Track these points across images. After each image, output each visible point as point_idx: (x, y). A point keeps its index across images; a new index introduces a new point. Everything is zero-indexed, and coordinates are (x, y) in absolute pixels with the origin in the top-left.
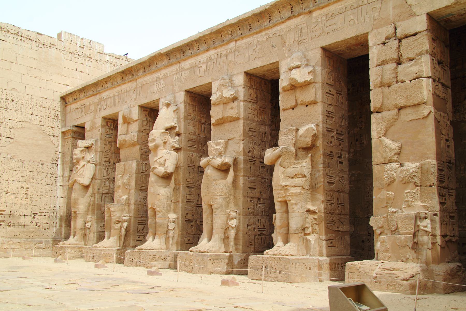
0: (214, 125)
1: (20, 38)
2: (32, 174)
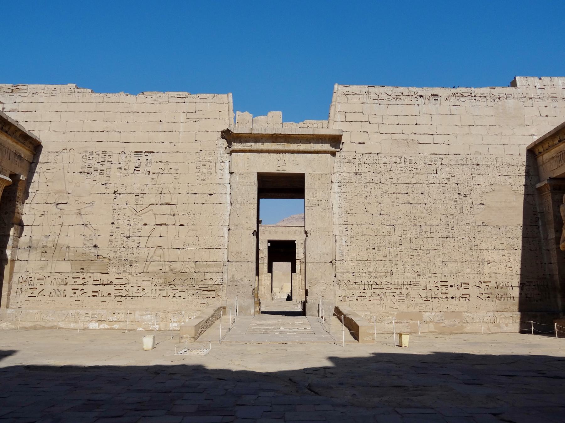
1: (474, 98)
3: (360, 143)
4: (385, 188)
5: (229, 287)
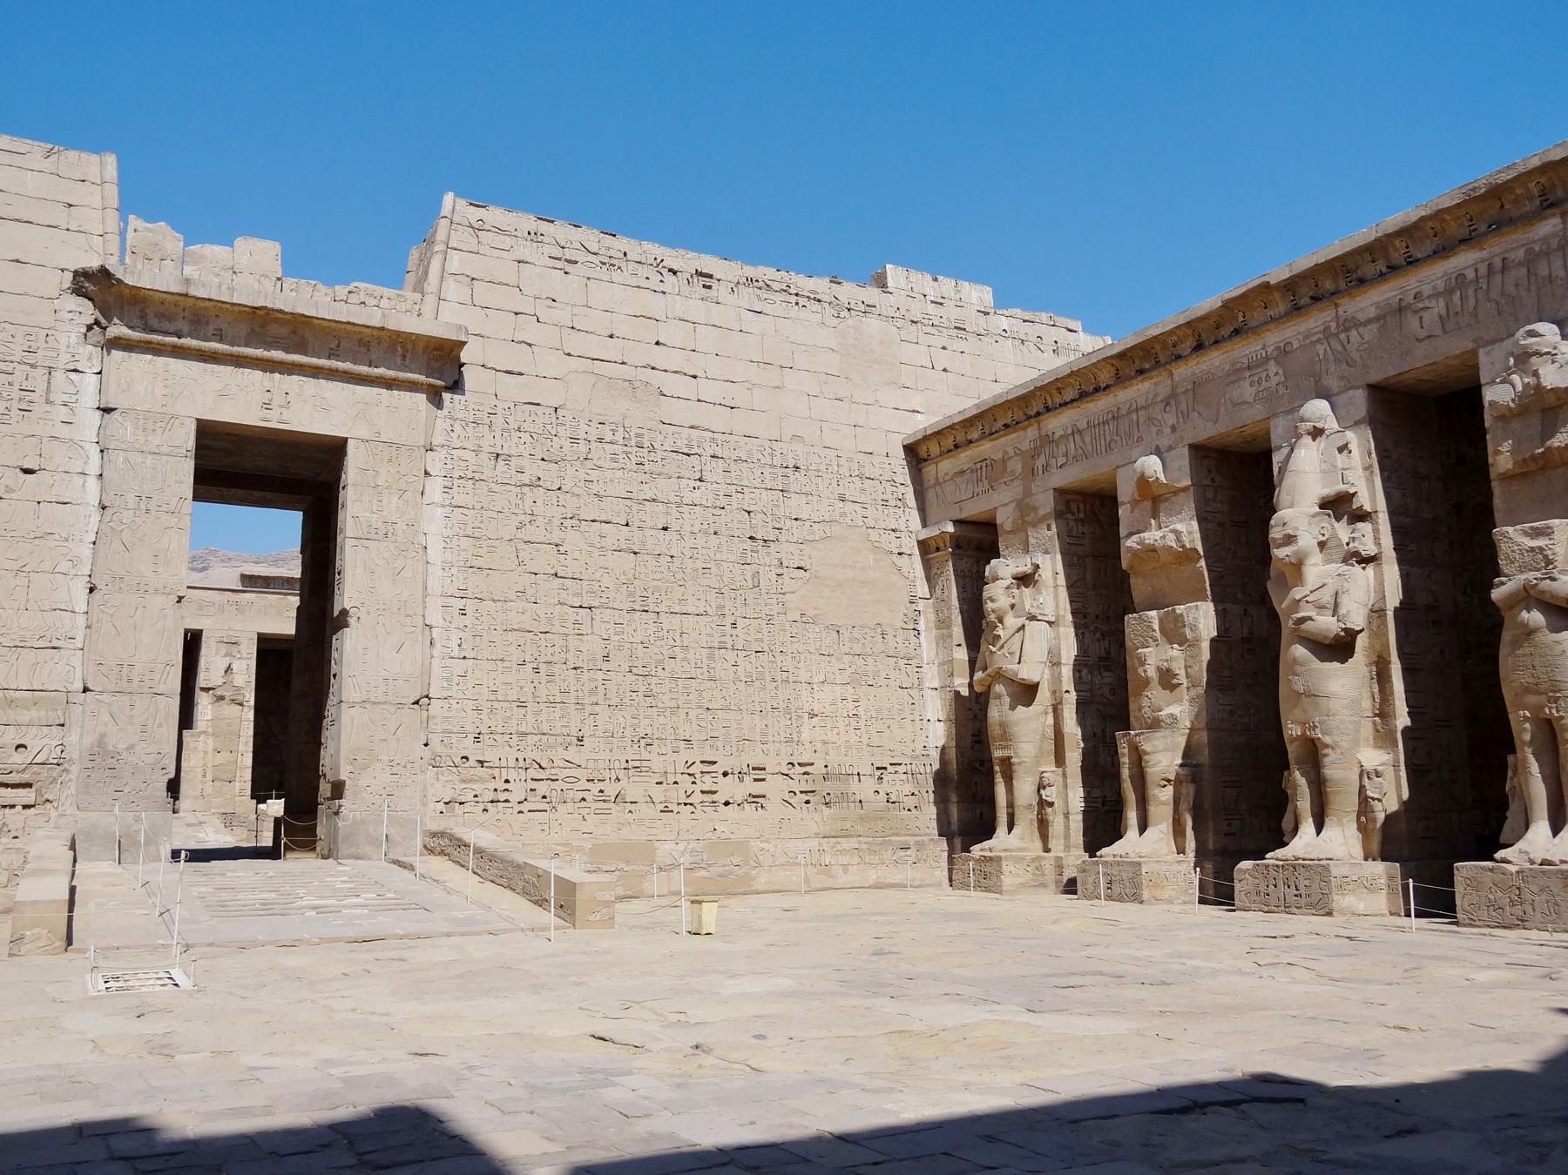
0: (1506, 477)
1: (793, 299)
2: (860, 662)
4: (571, 504)
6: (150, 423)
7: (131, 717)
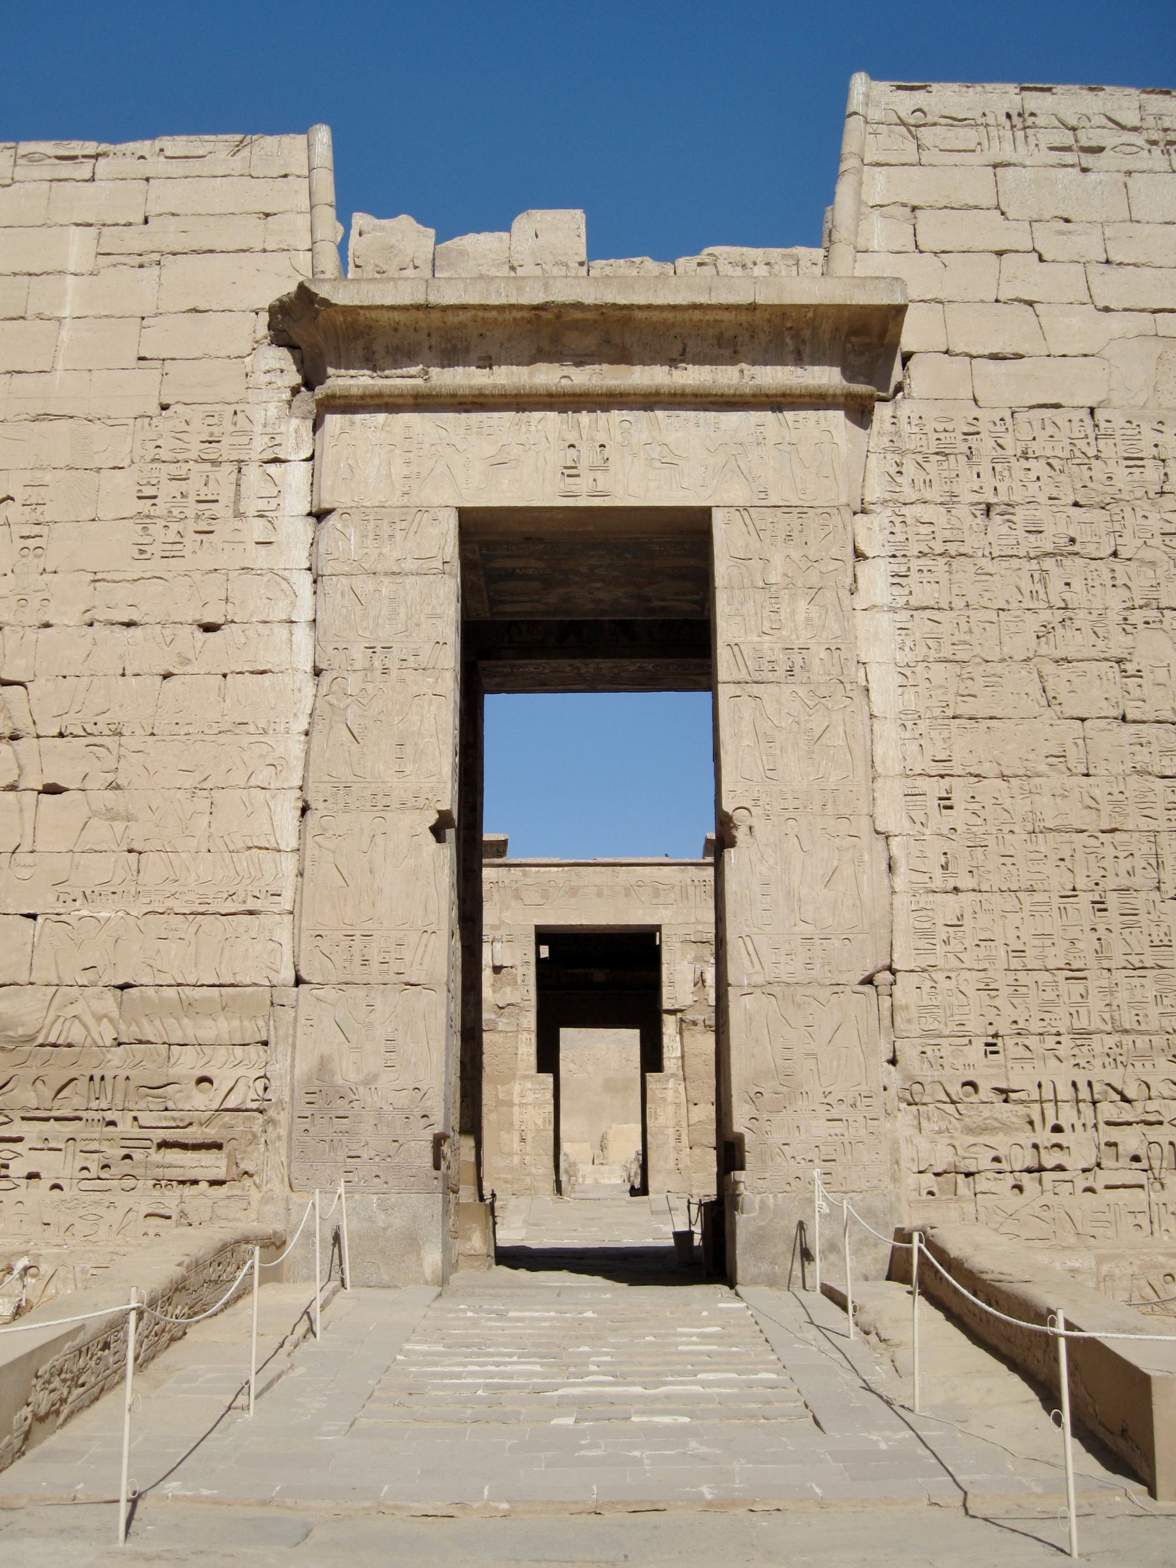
3: (994, 357)
4: (1141, 582)
5: (302, 1124)
6: (385, 525)
7: (369, 1026)
